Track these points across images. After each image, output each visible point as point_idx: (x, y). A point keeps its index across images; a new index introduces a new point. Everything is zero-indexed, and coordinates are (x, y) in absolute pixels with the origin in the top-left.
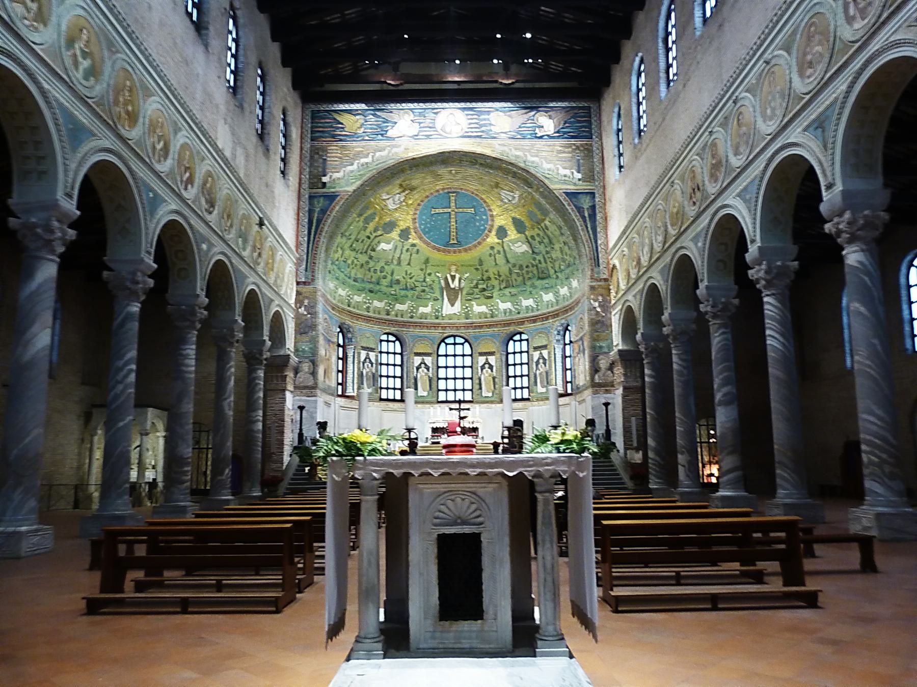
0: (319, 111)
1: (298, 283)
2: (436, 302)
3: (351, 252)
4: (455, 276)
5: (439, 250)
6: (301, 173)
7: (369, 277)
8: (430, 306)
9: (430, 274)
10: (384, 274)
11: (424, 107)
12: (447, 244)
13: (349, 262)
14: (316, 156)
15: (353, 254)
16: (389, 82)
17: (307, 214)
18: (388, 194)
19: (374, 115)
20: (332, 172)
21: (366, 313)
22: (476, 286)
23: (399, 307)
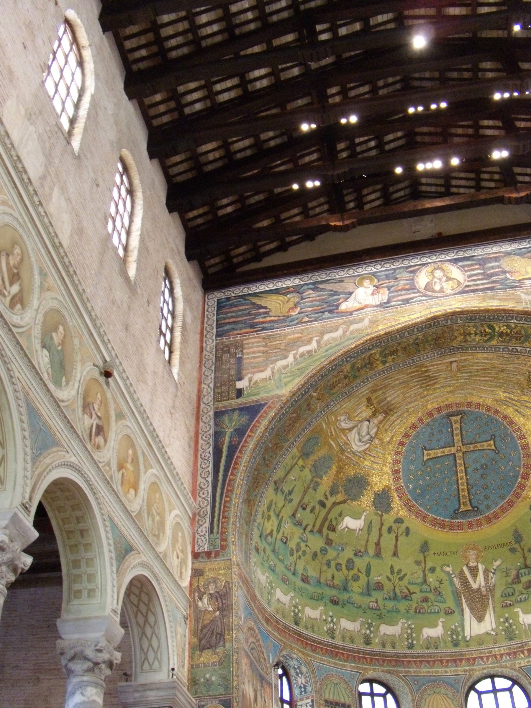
0: (228, 299)
1: (196, 556)
2: (449, 617)
3: (295, 529)
4: (476, 569)
5: (442, 525)
6: (200, 384)
7: (330, 578)
8: (440, 624)
9: (433, 570)
10: (355, 571)
11: (393, 267)
12: (456, 514)
13: (292, 544)
14: (226, 356)
15: (298, 531)
16: (332, 224)
17: (211, 441)
18: (349, 418)
19: (315, 289)
20: (253, 373)
21: (330, 640)
22: (517, 579)
23: (385, 629)
